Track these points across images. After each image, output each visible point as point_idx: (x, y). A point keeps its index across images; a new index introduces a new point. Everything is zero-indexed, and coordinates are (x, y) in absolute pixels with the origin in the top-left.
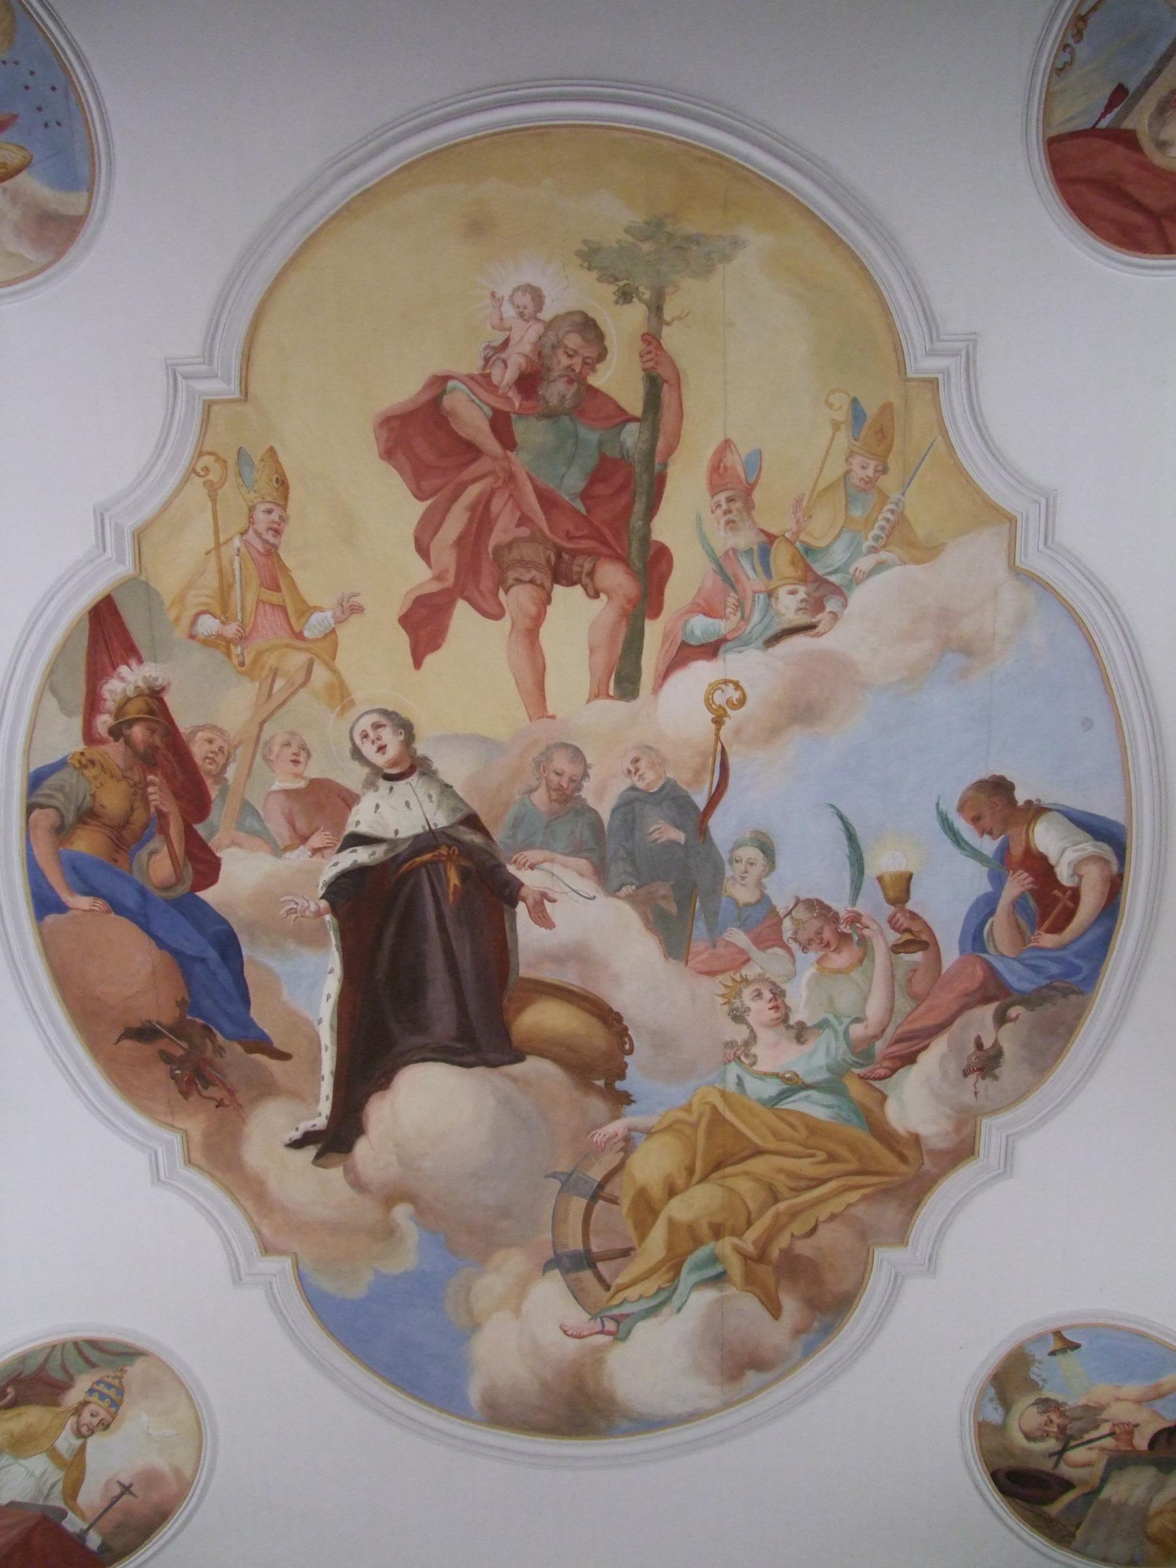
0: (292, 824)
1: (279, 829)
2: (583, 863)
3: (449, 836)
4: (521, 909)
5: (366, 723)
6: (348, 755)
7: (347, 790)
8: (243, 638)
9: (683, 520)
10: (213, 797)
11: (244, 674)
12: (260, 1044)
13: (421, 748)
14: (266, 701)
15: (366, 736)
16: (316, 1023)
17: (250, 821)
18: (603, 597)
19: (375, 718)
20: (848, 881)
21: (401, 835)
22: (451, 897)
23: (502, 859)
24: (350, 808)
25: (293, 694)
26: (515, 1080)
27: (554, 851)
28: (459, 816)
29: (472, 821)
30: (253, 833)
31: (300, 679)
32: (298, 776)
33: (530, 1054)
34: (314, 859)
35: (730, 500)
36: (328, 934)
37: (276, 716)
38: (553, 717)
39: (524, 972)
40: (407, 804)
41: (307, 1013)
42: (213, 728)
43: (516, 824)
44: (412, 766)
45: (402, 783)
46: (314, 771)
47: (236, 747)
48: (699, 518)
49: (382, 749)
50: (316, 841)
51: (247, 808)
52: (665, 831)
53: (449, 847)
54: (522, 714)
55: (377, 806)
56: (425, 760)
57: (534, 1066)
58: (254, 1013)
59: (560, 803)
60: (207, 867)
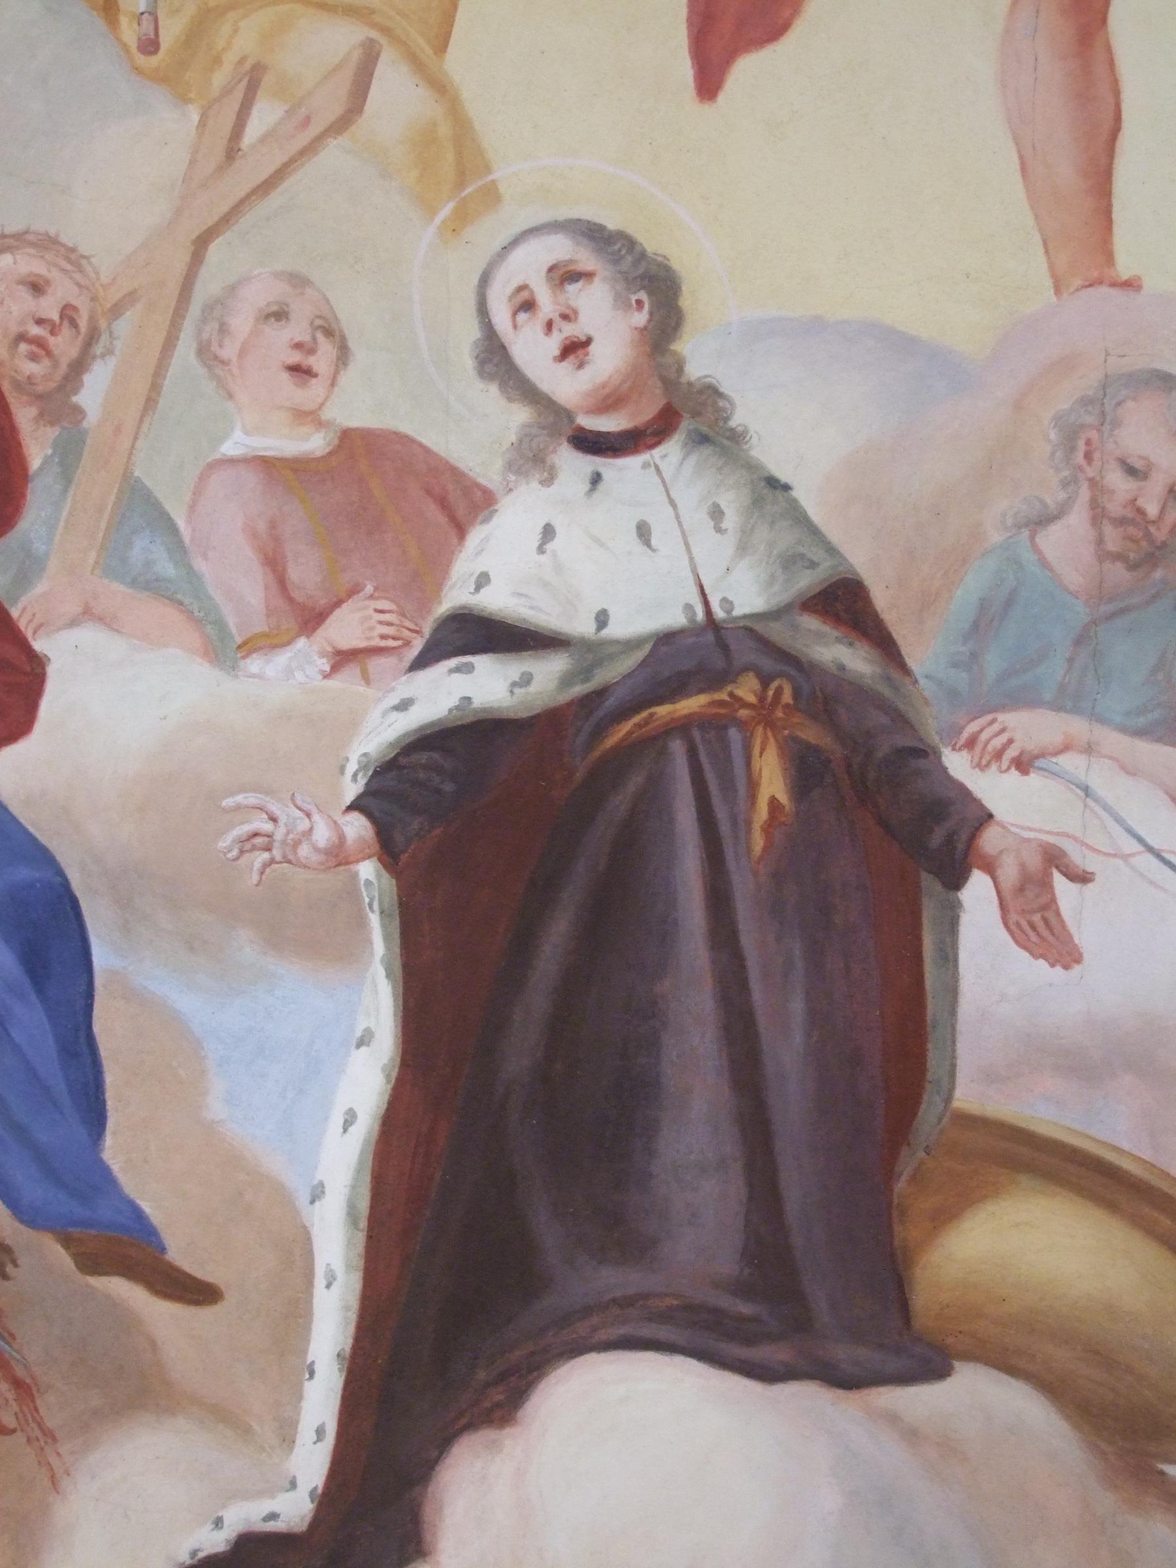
0: (274, 563)
1: (238, 587)
3: (766, 645)
4: (978, 892)
5: (529, 265)
6: (468, 363)
7: (456, 473)
10: (35, 463)
11: (160, 78)
12: (125, 1247)
13: (700, 356)
14: (220, 169)
15: (528, 306)
16: (303, 1198)
17: (147, 550)
19: (559, 248)
21: (617, 630)
22: (758, 842)
23: (932, 722)
24: (461, 531)
25: (310, 149)
26: (912, 1435)
27: (1102, 720)
28: (806, 581)
29: (843, 602)
30: (152, 586)
31: (330, 108)
32: (308, 417)
33: (969, 1357)
34: (334, 683)
36: (361, 923)
37: (245, 222)
38: (1131, 285)
39: (969, 1095)
40: (643, 532)
41: (275, 1163)
42: (47, 243)
43: (984, 623)
44: (666, 412)
45: (632, 463)
46: (357, 404)
47: (116, 311)
49: (574, 349)
50: (348, 626)
51: (139, 507)
53: (765, 684)
54: (1035, 268)
55: (548, 532)
56: (711, 393)
57: (972, 1395)
58: (115, 1151)
59: (1133, 567)
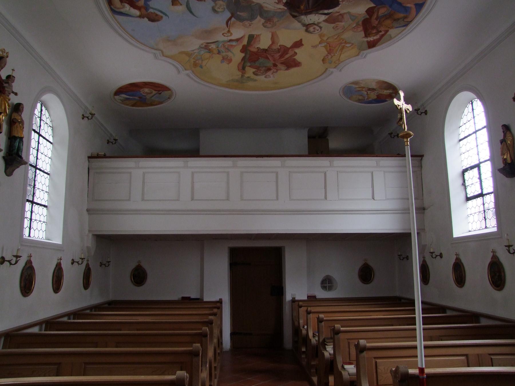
2: (266, 9)
8: (342, 43)
9: (238, 56)
20: (190, 3)
29: (294, 17)
52: (243, 14)
60: (370, 12)
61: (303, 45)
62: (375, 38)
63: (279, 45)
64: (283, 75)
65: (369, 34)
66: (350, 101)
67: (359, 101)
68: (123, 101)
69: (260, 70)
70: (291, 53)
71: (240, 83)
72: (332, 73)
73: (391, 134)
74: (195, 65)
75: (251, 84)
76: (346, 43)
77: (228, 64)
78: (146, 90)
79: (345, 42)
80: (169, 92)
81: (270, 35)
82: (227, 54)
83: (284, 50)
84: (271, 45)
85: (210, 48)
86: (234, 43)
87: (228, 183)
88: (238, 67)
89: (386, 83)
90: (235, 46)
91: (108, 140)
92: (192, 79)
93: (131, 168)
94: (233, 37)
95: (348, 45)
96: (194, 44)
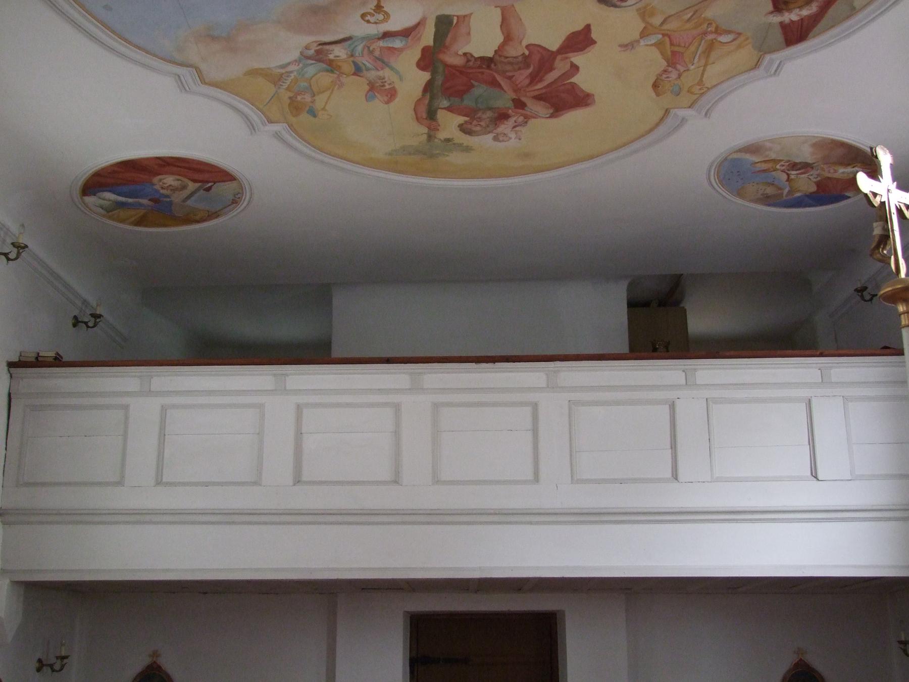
8: (705, 33)
9: (412, 80)
18: (460, 53)
35: (384, 86)
48: (401, 79)
61: (593, 42)
62: (805, 12)
63: (525, 43)
64: (544, 132)
65: (786, 3)
66: (739, 201)
67: (767, 200)
68: (111, 210)
69: (480, 119)
70: (561, 67)
71: (426, 157)
72: (684, 120)
73: (861, 291)
74: (296, 107)
75: (456, 158)
76: (718, 31)
77: (387, 103)
78: (170, 180)
79: (717, 28)
80: (232, 185)
81: (497, 15)
82: (381, 73)
83: (541, 60)
84: (502, 47)
85: (331, 57)
86: (397, 43)
87: (397, 433)
88: (415, 110)
89: (842, 144)
90: (400, 50)
91: (75, 317)
92: (291, 146)
93: (128, 394)
94: (395, 24)
95: (724, 39)
96: (286, 48)
